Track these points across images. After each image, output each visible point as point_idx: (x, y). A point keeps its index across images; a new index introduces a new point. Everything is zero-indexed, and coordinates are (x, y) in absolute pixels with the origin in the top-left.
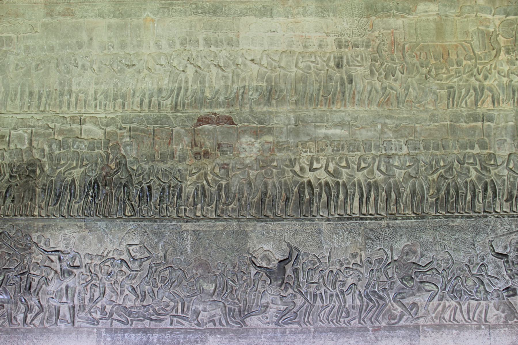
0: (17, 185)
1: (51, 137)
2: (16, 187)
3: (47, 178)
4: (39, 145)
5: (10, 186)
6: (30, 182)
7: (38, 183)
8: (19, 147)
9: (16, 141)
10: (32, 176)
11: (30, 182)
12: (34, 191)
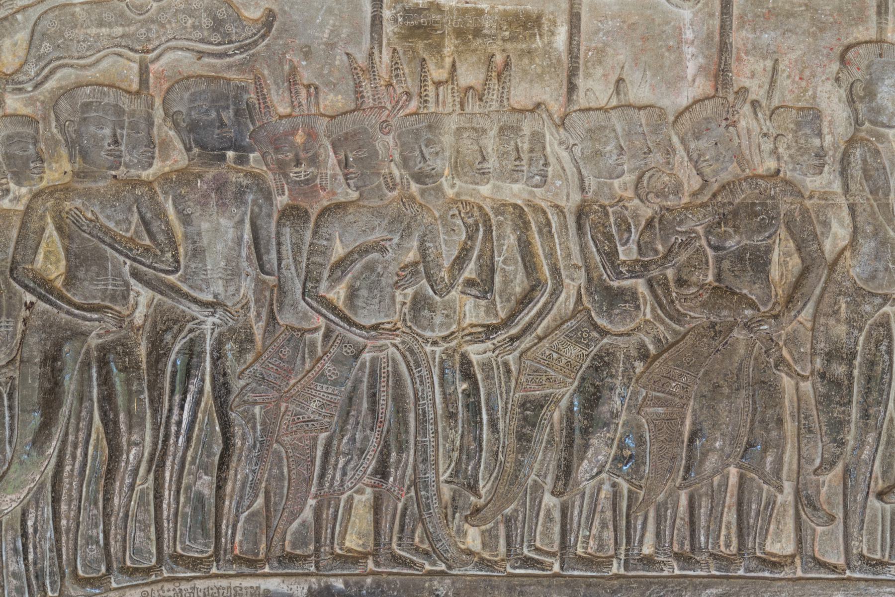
0: (644, 355)
1: (860, 33)
2: (639, 366)
3: (855, 304)
4: (783, 81)
5: (602, 363)
6: (739, 335)
7: (793, 340)
8: (640, 91)
9: (621, 54)
10: (751, 291)
11: (739, 335)
12: (767, 390)
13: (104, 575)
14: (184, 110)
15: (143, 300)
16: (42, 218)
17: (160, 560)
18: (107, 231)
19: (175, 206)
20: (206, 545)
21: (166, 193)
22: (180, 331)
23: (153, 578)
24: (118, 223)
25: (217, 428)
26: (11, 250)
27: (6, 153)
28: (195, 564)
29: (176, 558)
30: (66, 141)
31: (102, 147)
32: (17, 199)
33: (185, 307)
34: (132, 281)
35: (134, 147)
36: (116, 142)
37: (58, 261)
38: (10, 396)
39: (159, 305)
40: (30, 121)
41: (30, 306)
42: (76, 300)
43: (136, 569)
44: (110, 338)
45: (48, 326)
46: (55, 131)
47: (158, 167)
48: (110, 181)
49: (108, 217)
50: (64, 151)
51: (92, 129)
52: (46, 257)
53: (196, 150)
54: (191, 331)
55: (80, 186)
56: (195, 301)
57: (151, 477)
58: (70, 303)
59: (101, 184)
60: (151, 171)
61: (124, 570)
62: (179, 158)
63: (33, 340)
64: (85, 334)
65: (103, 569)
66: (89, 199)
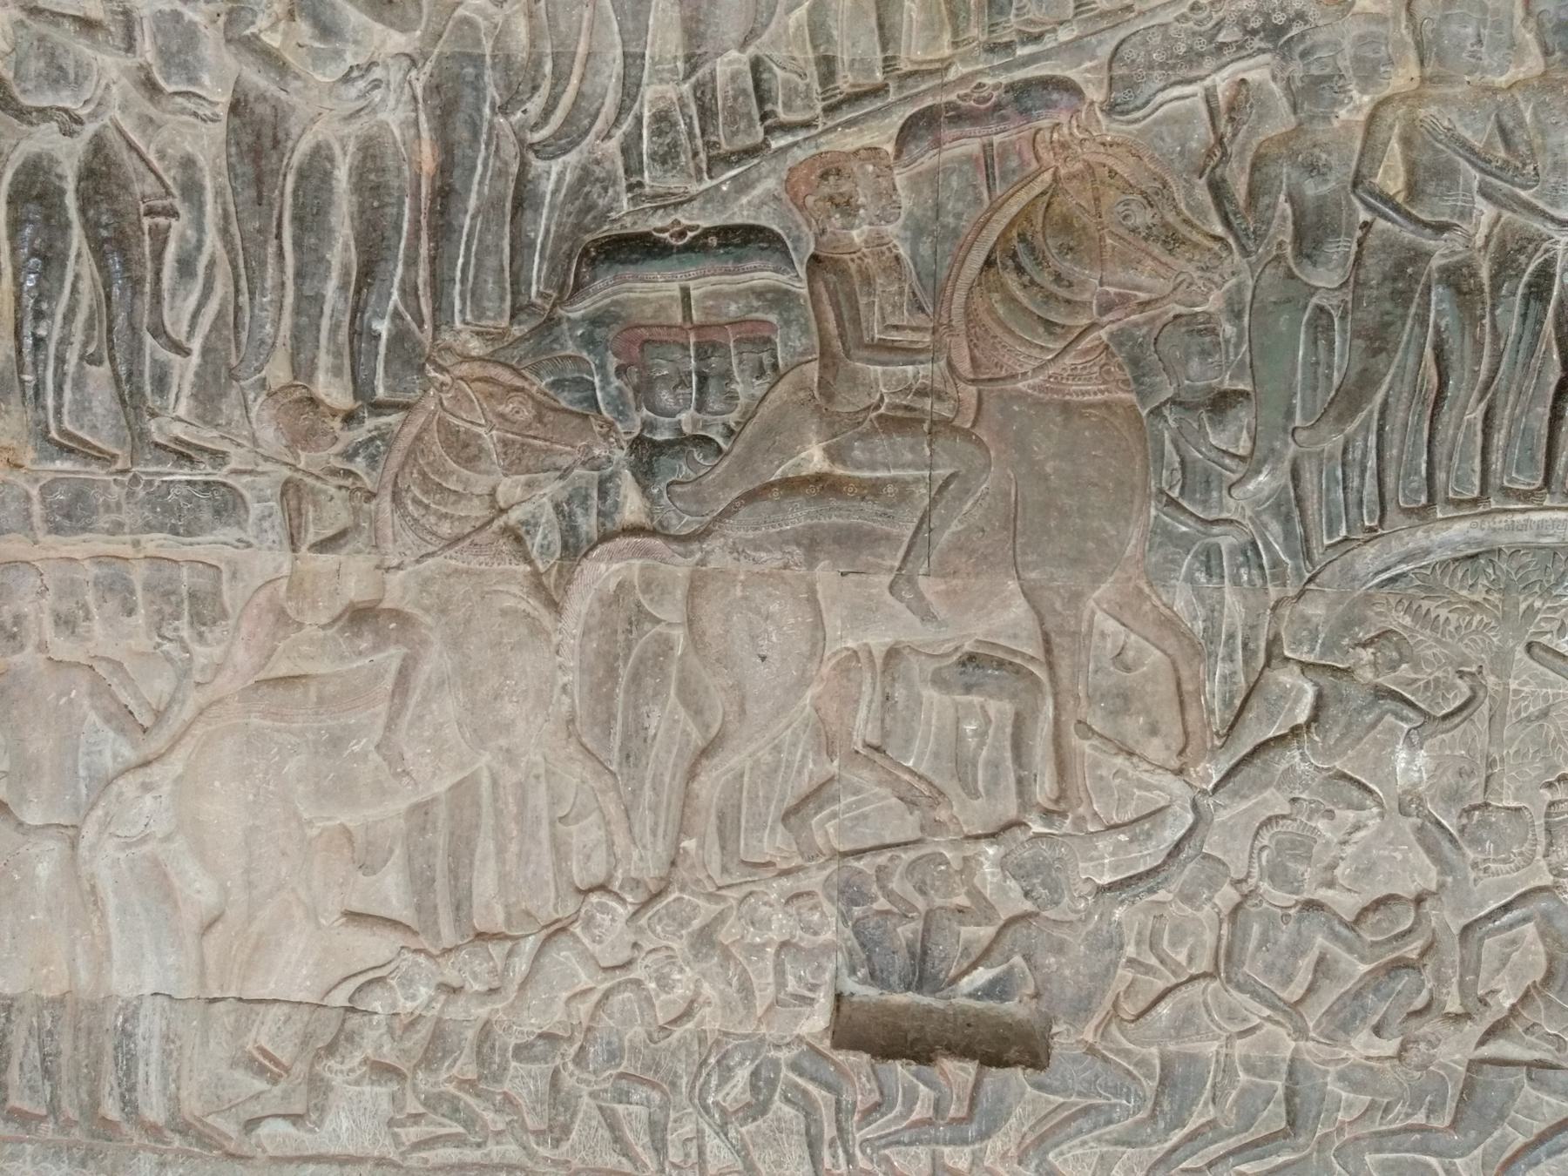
13: (1424, 507)
14: (1552, 9)
15: (1485, 220)
16: (1391, 127)
17: (1483, 490)
18: (1464, 144)
19: (1535, 114)
20: (1532, 477)
21: (1528, 100)
22: (1536, 250)
23: (1481, 509)
24: (1475, 132)
25: (1555, 357)
26: (1354, 164)
27: (1355, 56)
28: (1525, 496)
29: (1507, 492)
30: (1419, 45)
31: (1463, 49)
32: (1358, 108)
33: (1537, 225)
34: (1478, 198)
35: (1496, 49)
36: (1480, 42)
37: (1397, 176)
38: (1343, 318)
39: (1508, 223)
40: (1381, 19)
41: (1366, 226)
42: (1425, 217)
43: (1462, 501)
44: (1456, 258)
45: (1389, 245)
46: (1404, 32)
47: (1513, 74)
48: (1466, 87)
49: (1466, 126)
50: (1412, 55)
51: (1454, 28)
52: (1385, 172)
53: (1558, 55)
54: (1547, 251)
55: (1433, 92)
56: (1553, 219)
57: (1483, 406)
58: (1417, 221)
59: (1458, 90)
60: (1503, 79)
61: (1448, 501)
62: (1533, 63)
63: (1369, 261)
64: (1429, 255)
65: (1424, 499)
66: (1446, 106)
